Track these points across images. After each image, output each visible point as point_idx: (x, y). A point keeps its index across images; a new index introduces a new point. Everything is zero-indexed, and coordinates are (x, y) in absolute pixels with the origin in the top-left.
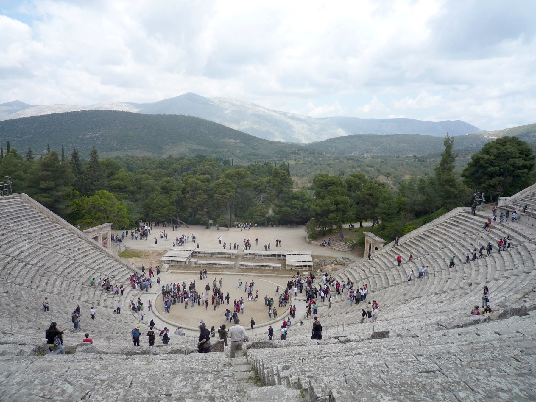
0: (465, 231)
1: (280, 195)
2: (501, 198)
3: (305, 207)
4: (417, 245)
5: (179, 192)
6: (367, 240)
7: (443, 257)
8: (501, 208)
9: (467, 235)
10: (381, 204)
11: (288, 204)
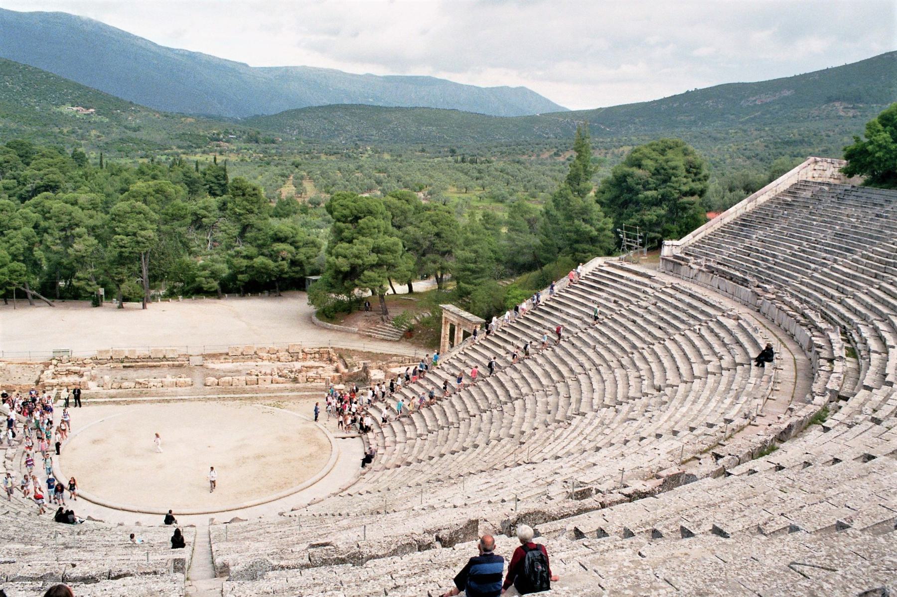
0: (617, 299)
1: (248, 235)
2: (666, 242)
3: (301, 257)
4: (539, 324)
5: (28, 230)
6: (446, 318)
7: (592, 344)
8: (666, 259)
9: (621, 306)
10: (459, 253)
11: (265, 251)
